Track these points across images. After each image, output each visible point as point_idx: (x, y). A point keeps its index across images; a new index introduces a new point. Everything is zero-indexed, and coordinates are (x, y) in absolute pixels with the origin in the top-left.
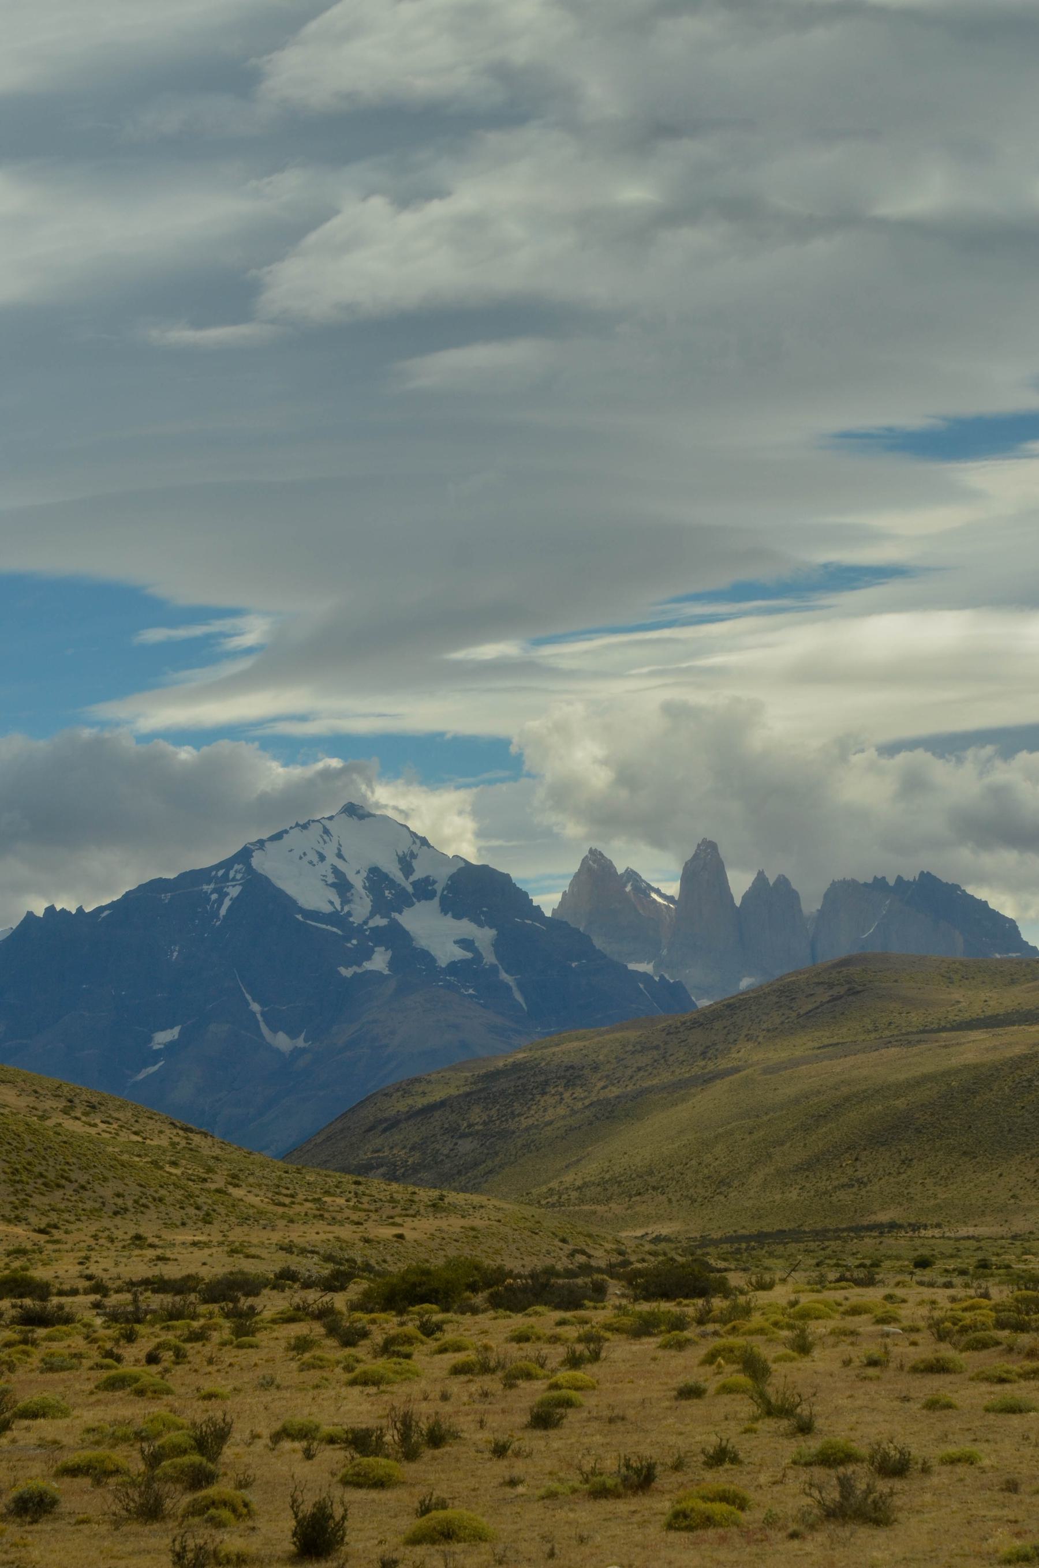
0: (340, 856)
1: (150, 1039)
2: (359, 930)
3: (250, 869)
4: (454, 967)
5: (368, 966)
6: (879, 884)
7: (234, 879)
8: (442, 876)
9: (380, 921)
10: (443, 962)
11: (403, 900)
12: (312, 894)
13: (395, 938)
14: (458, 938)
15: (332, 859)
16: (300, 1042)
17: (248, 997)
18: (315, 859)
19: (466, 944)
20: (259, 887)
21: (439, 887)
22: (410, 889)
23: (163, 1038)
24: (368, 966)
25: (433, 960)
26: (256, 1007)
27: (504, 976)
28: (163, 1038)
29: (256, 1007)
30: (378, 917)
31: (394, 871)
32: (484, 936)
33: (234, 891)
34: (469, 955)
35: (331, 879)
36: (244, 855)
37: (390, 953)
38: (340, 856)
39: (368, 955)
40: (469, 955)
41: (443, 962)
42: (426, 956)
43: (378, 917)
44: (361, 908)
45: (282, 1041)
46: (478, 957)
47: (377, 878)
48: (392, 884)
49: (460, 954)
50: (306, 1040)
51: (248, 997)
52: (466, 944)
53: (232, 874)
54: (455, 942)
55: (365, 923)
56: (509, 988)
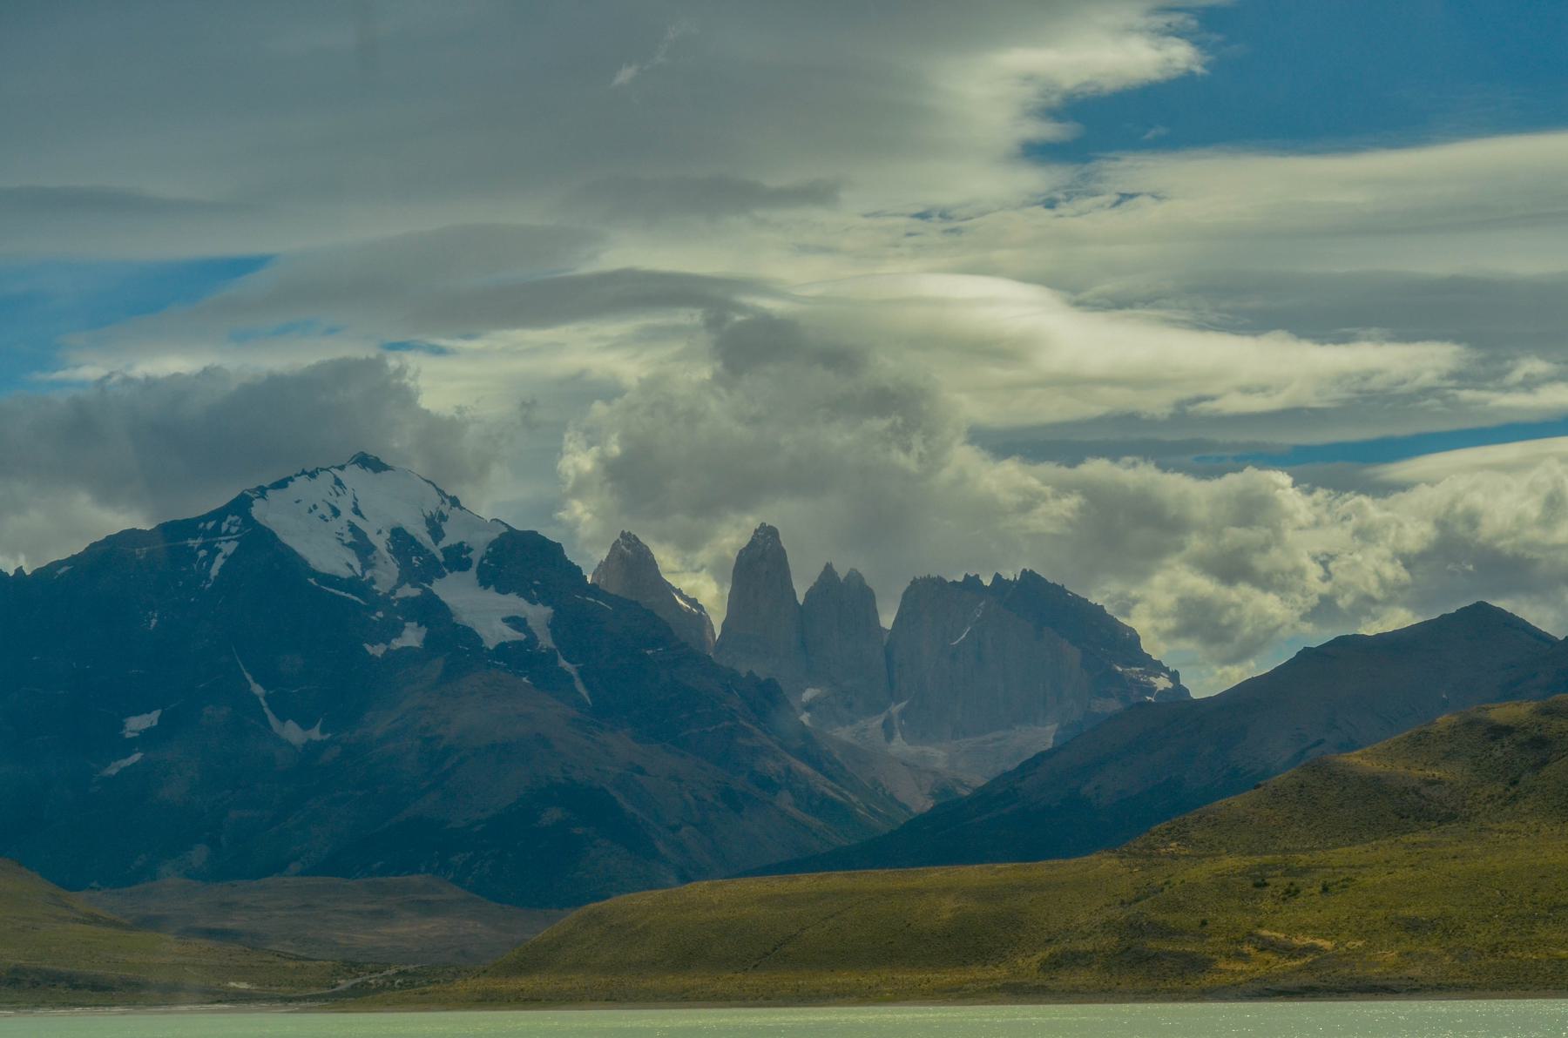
0: (357, 511)
1: (122, 726)
2: (385, 601)
3: (248, 520)
4: (503, 650)
5: (397, 644)
6: (972, 583)
7: (227, 533)
8: (479, 543)
9: (410, 591)
10: (490, 643)
11: (432, 569)
12: (326, 555)
13: (430, 611)
14: (505, 615)
15: (347, 514)
16: (315, 734)
17: (248, 677)
18: (328, 513)
19: (516, 622)
20: (259, 540)
21: (476, 556)
22: (440, 557)
23: (137, 724)
24: (397, 644)
25: (479, 640)
26: (258, 689)
27: (563, 663)
28: (137, 724)
29: (258, 689)
30: (407, 586)
31: (421, 533)
32: (538, 615)
33: (229, 548)
34: (521, 636)
35: (348, 538)
36: (241, 505)
37: (424, 630)
38: (357, 511)
39: (397, 630)
40: (521, 636)
41: (490, 643)
42: (469, 636)
43: (407, 586)
44: (386, 574)
45: (293, 733)
46: (532, 639)
47: (401, 541)
48: (419, 549)
49: (511, 635)
50: (323, 732)
51: (248, 677)
52: (516, 622)
53: (224, 527)
54: (505, 620)
55: (393, 592)
56: (571, 678)
